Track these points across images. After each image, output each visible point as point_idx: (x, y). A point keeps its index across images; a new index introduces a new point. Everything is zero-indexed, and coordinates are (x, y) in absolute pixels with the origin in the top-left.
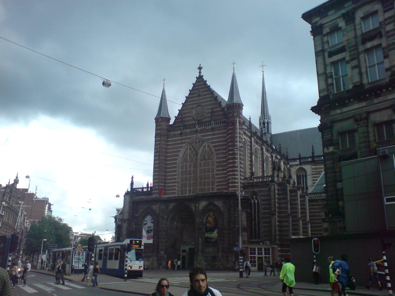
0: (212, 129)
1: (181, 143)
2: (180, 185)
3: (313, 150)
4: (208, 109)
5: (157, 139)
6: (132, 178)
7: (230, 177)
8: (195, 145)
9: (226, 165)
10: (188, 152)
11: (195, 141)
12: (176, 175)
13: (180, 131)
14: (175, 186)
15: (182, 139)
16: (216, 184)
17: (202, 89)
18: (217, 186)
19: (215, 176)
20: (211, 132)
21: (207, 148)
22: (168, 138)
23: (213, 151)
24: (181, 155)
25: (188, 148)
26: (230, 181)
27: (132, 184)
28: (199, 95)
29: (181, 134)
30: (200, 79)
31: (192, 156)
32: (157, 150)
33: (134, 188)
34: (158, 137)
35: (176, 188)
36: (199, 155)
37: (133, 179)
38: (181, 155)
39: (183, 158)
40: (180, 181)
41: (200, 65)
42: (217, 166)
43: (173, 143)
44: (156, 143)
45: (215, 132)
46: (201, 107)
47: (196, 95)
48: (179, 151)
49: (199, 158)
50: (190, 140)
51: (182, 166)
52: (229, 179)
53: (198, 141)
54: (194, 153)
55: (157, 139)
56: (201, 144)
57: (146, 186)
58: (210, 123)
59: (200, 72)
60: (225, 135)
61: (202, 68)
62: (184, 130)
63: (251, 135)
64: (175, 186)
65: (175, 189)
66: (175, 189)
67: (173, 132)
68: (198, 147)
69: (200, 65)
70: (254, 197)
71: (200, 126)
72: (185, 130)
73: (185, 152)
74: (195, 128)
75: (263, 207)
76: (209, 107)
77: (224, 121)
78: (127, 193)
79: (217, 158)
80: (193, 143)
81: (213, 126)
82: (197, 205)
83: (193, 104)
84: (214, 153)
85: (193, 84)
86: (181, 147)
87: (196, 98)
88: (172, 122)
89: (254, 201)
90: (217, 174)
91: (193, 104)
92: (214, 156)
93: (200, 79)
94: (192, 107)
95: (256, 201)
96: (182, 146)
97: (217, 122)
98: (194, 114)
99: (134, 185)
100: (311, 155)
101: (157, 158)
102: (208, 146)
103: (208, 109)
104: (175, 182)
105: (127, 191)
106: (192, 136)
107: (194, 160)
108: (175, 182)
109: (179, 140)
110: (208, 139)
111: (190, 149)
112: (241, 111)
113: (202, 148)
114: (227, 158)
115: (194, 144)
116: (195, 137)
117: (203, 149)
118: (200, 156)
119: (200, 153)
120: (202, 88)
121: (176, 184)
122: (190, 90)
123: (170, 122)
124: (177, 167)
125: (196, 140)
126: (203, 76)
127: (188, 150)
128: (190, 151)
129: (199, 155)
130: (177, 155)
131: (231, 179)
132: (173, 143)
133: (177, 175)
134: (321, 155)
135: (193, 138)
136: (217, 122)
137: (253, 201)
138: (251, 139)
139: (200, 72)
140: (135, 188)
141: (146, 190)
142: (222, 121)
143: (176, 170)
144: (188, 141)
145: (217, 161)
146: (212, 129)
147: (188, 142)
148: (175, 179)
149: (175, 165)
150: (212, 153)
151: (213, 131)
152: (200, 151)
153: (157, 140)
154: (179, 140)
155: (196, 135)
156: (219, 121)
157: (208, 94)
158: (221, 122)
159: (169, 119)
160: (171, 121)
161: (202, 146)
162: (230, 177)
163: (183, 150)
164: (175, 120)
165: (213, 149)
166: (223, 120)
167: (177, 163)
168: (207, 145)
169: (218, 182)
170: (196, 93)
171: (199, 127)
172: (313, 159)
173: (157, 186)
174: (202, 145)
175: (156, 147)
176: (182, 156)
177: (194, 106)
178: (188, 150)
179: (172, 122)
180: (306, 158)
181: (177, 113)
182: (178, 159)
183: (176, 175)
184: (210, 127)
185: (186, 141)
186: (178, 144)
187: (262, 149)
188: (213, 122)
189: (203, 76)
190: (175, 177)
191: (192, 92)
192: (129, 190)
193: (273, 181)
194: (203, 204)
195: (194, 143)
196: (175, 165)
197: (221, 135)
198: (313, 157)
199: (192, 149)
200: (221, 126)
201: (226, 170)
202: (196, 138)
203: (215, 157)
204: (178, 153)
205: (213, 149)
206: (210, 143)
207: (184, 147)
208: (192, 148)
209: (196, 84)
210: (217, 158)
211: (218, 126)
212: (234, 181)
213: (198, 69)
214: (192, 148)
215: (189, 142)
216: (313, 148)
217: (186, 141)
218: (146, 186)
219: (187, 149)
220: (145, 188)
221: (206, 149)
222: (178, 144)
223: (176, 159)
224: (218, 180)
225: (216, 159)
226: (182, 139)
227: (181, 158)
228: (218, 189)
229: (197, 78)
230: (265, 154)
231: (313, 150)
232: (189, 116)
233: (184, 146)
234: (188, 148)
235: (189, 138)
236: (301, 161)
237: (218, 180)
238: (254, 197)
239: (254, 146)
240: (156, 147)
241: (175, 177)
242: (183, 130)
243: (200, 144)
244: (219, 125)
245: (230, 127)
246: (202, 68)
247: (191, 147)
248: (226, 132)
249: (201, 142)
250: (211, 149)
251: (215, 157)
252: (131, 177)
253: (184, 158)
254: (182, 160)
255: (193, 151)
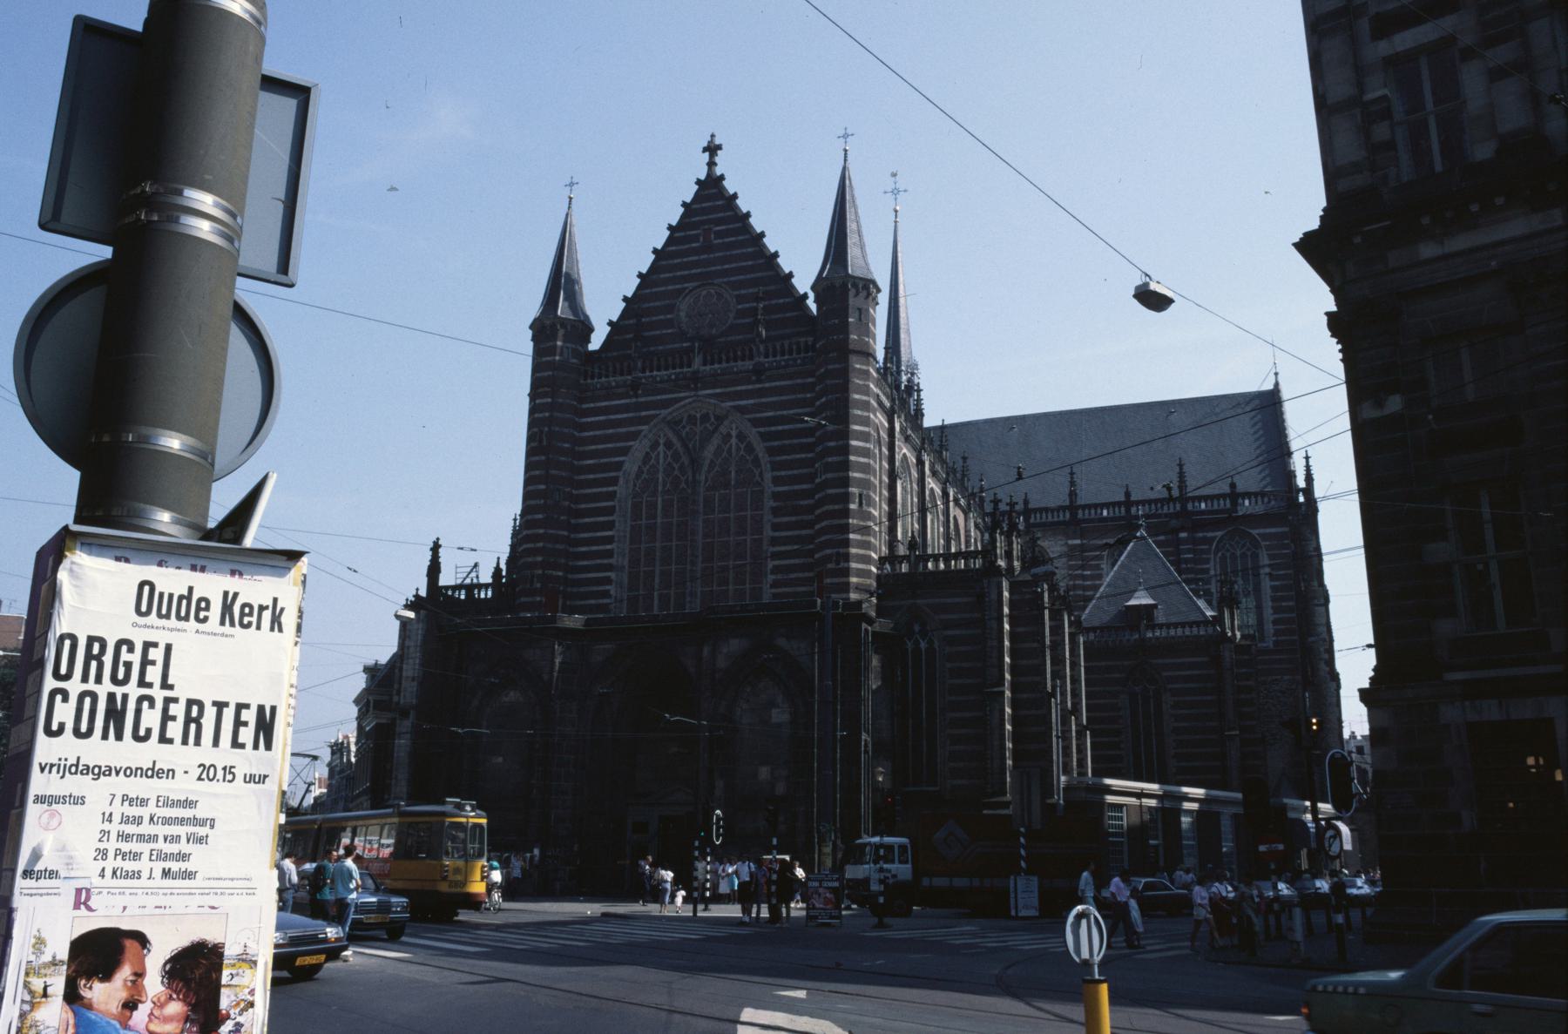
0: (759, 372)
1: (630, 422)
2: (626, 580)
3: (1072, 483)
4: (740, 299)
5: (537, 401)
6: (436, 548)
7: (828, 551)
8: (687, 429)
9: (811, 509)
10: (662, 455)
11: (690, 416)
12: (610, 540)
13: (629, 377)
14: (608, 581)
15: (639, 407)
16: (771, 578)
17: (717, 225)
18: (775, 585)
19: (765, 548)
20: (753, 383)
21: (734, 441)
22: (582, 400)
23: (760, 455)
24: (631, 464)
25: (662, 441)
26: (830, 566)
27: (434, 569)
28: (709, 248)
29: (635, 386)
30: (711, 187)
31: (676, 472)
32: (541, 441)
33: (442, 583)
34: (545, 395)
35: (612, 589)
36: (705, 468)
37: (440, 550)
38: (631, 464)
39: (638, 476)
40: (626, 563)
41: (713, 136)
42: (775, 512)
43: (602, 418)
44: (536, 415)
45: (767, 385)
46: (712, 291)
47: (694, 245)
48: (625, 451)
49: (703, 478)
50: (670, 410)
51: (636, 507)
52: (828, 559)
53: (698, 415)
54: (685, 460)
55: (537, 401)
56: (711, 428)
57: (490, 581)
58: (751, 350)
59: (711, 164)
60: (809, 395)
61: (719, 147)
62: (648, 374)
63: (892, 407)
64: (608, 581)
65: (609, 591)
66: (606, 594)
67: (603, 379)
68: (697, 438)
69: (713, 136)
70: (917, 628)
71: (709, 358)
72: (651, 371)
73: (647, 453)
74: (689, 366)
75: (949, 665)
76: (743, 292)
77: (806, 342)
78: (416, 604)
79: (777, 481)
80: (681, 421)
81: (762, 359)
82: (706, 651)
83: (685, 279)
84: (764, 458)
85: (684, 204)
86: (634, 436)
87: (695, 258)
88: (596, 342)
89: (917, 643)
90: (774, 541)
91: (685, 279)
92: (761, 474)
93: (711, 187)
94: (678, 290)
95: (923, 645)
96: (641, 431)
97: (778, 347)
98: (682, 314)
99: (441, 576)
100: (1064, 500)
101: (537, 472)
102: (737, 436)
103: (740, 299)
104: (610, 568)
105: (417, 596)
106: (682, 395)
107: (683, 485)
108: (610, 568)
109: (626, 408)
110: (742, 410)
111: (668, 445)
112: (871, 311)
113: (716, 441)
114: (818, 481)
115: (684, 427)
116: (690, 400)
117: (719, 447)
118: (709, 471)
119: (707, 462)
120: (719, 222)
121: (612, 575)
122: (670, 228)
123: (589, 342)
124: (617, 508)
125: (693, 413)
126: (722, 177)
127: (661, 448)
128: (669, 453)
129: (705, 468)
130: (619, 466)
131: (834, 558)
132: (602, 418)
133: (616, 539)
134: (1117, 499)
135: (682, 403)
136: (778, 347)
137: (910, 645)
138: (891, 422)
139: (711, 164)
140: (447, 588)
141: (490, 594)
142: (798, 343)
143: (614, 521)
144: (664, 412)
145: (773, 493)
146: (759, 372)
147: (661, 416)
148: (610, 554)
149: (610, 503)
150: (756, 461)
151: (759, 381)
152: (709, 452)
153: (539, 404)
154: (626, 408)
155: (693, 393)
156: (786, 343)
157: (742, 244)
158: (794, 347)
159: (586, 329)
160: (593, 336)
161: (716, 435)
162: (828, 551)
163: (639, 447)
164: (609, 336)
165: (760, 448)
166: (803, 340)
167: (618, 495)
168: (734, 433)
169: (776, 570)
170: (695, 238)
171: (705, 364)
172: (1074, 515)
173: (535, 579)
174: (716, 429)
175: (535, 430)
176: (635, 468)
177: (686, 285)
178: (661, 448)
179: (596, 342)
180: (1046, 510)
181: (615, 310)
182: (621, 481)
183: (610, 540)
184: (749, 365)
185: (658, 412)
186: (620, 423)
187: (920, 463)
188: (762, 348)
189: (722, 177)
190: (609, 547)
191: (677, 235)
192: (423, 593)
193: (991, 570)
194: (735, 645)
195: (684, 423)
196: (610, 503)
197: (793, 397)
198: (1073, 507)
199: (678, 445)
200: (795, 360)
201: (810, 525)
202: (690, 403)
203: (768, 476)
204: (621, 459)
205: (760, 448)
206: (749, 424)
207: (645, 436)
208: (675, 440)
209: (695, 206)
210: (777, 481)
211: (783, 363)
212: (842, 565)
213: (705, 150)
214: (675, 440)
215: (665, 418)
216: (1072, 478)
217: (658, 412)
218: (490, 581)
219: (655, 445)
220: (486, 586)
221: (731, 445)
222: (620, 423)
223: (614, 481)
224: (777, 563)
225: (770, 485)
226: (639, 407)
227: (633, 476)
228: (775, 596)
229: (699, 182)
230: (929, 483)
231: (1072, 483)
232: (670, 323)
233: (643, 434)
234: (662, 441)
235: (665, 404)
236: (1032, 520)
237: (777, 563)
238: (917, 628)
239: (901, 449)
240: (535, 430)
241: (609, 547)
242: (644, 372)
243: (706, 427)
244: (786, 357)
245: (830, 367)
246: (719, 147)
247: (671, 435)
248: (812, 383)
249: (713, 419)
250: (750, 449)
251: (768, 476)
252: (432, 545)
253: (645, 476)
254: (635, 485)
255: (681, 450)
